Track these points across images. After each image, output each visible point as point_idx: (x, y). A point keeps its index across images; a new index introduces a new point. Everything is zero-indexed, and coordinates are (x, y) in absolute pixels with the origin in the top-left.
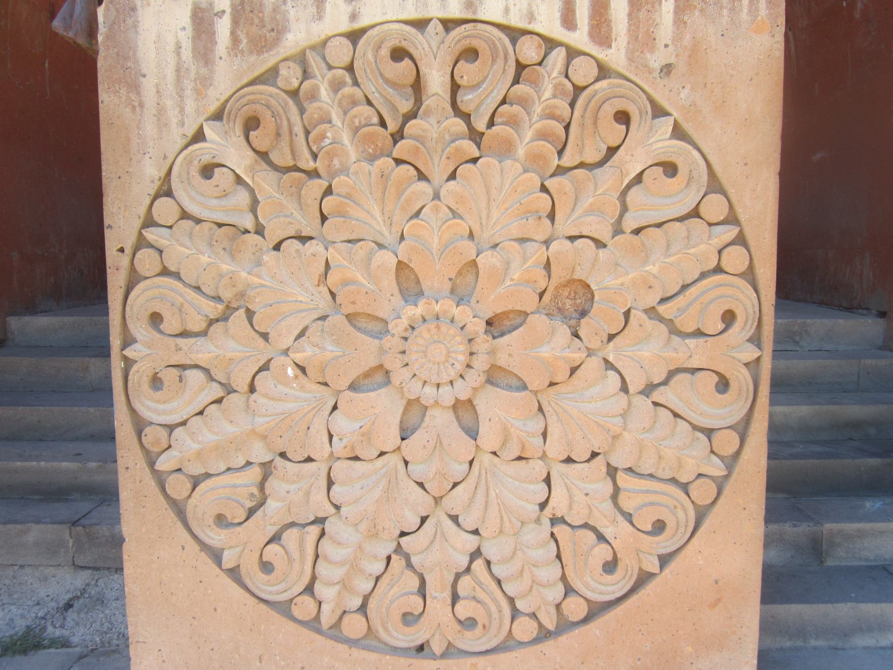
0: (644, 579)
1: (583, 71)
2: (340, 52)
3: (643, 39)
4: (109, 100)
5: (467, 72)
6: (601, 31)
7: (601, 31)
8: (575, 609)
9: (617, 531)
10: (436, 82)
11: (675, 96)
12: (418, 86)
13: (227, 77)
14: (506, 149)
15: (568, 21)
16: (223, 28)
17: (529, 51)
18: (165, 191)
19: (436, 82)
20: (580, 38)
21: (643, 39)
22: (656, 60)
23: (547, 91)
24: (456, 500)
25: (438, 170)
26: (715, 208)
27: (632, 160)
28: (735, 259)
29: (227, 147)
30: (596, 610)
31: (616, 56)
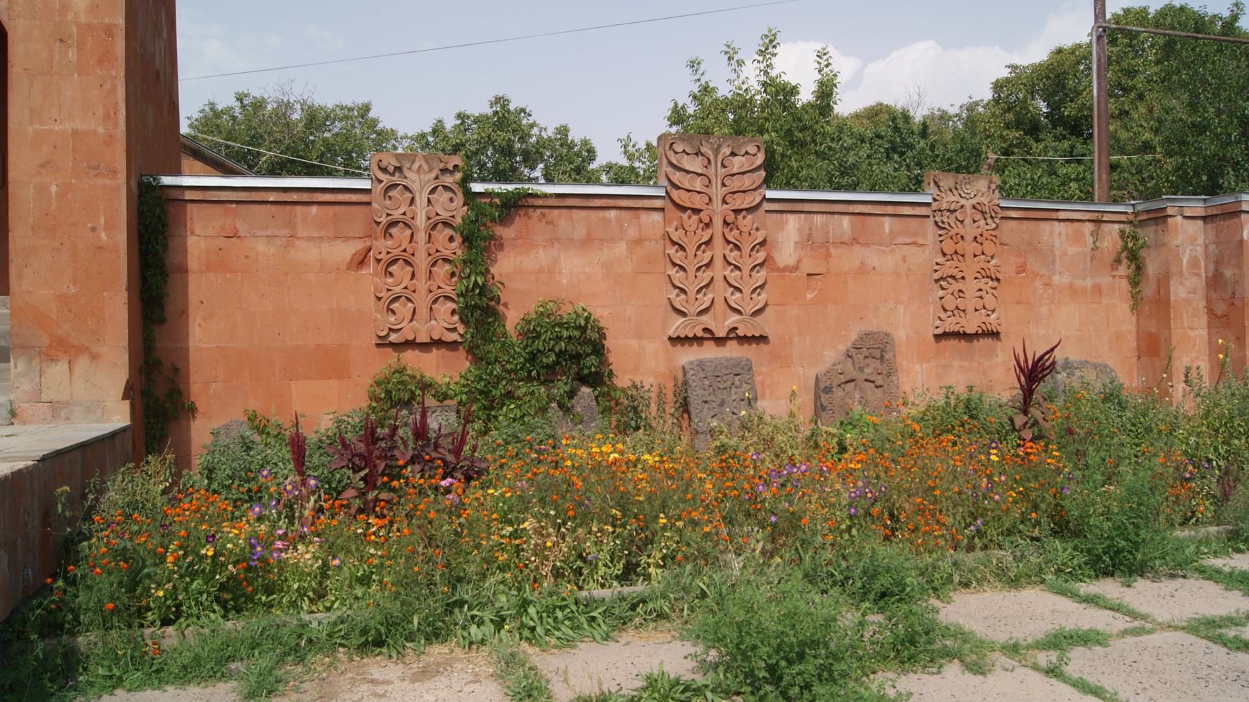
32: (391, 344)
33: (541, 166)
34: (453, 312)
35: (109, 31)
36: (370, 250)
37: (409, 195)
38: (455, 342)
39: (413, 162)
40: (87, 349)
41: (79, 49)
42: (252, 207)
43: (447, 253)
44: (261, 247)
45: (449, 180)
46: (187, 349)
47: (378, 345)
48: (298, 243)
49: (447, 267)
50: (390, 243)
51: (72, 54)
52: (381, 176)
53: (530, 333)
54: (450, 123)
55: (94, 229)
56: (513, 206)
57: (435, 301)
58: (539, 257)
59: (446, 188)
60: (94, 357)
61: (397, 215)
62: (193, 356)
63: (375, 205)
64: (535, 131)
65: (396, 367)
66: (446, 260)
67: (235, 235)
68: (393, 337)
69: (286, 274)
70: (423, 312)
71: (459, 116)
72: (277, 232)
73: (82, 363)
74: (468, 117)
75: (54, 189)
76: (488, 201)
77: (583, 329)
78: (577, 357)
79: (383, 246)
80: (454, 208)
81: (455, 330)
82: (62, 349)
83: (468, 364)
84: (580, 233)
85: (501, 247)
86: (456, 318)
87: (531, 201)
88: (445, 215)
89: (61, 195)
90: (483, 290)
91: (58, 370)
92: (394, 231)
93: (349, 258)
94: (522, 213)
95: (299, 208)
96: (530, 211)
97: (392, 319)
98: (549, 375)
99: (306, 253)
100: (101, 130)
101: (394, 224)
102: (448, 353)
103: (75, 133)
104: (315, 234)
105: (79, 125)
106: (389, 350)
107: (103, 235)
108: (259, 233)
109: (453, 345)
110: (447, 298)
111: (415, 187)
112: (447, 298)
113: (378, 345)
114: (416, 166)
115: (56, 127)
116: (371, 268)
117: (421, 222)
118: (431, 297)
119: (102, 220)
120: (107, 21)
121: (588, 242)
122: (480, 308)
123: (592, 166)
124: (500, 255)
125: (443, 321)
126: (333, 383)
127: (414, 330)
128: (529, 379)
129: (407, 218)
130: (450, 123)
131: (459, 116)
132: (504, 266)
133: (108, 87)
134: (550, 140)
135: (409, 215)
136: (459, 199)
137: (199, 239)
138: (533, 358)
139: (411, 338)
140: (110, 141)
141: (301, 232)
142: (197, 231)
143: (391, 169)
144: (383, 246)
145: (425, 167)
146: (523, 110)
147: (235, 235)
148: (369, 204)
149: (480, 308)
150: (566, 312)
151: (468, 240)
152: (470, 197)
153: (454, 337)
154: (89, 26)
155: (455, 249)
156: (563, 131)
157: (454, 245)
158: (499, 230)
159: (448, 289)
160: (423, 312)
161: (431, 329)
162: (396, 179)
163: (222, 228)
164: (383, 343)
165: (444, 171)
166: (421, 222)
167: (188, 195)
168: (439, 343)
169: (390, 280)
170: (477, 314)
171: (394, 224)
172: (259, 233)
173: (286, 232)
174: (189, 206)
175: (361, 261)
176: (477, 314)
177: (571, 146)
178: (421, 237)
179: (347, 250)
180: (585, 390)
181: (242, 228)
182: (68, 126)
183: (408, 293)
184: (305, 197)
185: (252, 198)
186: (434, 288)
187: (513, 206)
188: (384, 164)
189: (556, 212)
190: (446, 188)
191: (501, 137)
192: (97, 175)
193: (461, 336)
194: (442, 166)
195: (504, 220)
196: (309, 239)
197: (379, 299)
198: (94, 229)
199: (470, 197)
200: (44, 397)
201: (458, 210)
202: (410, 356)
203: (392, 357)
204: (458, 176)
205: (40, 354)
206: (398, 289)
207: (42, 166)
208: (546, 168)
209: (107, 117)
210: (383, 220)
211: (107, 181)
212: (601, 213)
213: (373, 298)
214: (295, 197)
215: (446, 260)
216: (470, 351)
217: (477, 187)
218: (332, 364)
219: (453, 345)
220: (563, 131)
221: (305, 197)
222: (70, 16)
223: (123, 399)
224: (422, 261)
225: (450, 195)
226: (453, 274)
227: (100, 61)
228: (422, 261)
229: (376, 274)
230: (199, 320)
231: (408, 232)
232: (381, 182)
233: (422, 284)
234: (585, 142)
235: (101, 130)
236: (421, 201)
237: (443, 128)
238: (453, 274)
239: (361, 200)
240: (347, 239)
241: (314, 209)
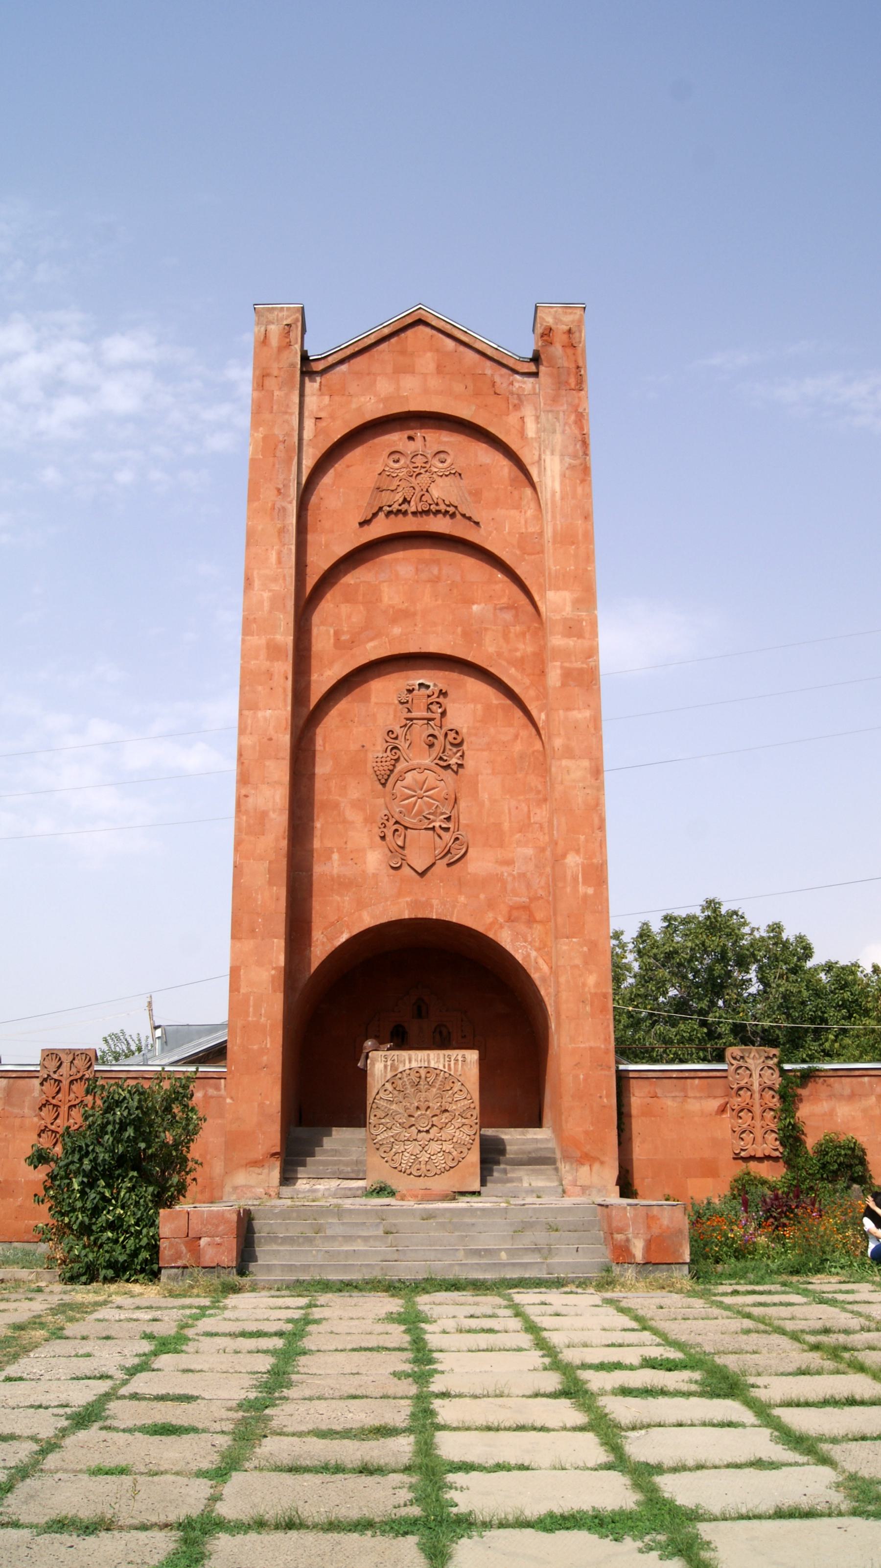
0: (459, 1161)
1: (447, 1075)
2: (408, 1072)
3: (456, 1070)
4: (369, 1079)
5: (428, 1075)
6: (450, 1069)
7: (450, 1069)
8: (447, 1168)
9: (455, 1153)
10: (423, 1076)
11: (461, 1079)
12: (420, 1077)
13: (389, 1077)
14: (435, 1087)
15: (444, 1067)
16: (389, 1068)
17: (438, 1072)
18: (378, 1093)
19: (423, 1076)
20: (446, 1070)
21: (456, 1070)
22: (459, 1073)
23: (440, 1079)
24: (426, 1149)
25: (423, 1091)
26: (469, 1098)
27: (456, 1089)
28: (472, 1106)
29: (388, 1086)
30: (451, 1167)
31: (452, 1073)
32: (742, 1158)
33: (754, 967)
34: (776, 1139)
35: (605, 996)
36: (727, 1103)
37: (748, 1072)
38: (778, 1157)
39: (750, 1053)
40: (598, 1159)
41: (592, 1006)
42: (664, 1080)
43: (771, 1105)
44: (670, 1103)
45: (771, 1063)
46: (632, 1160)
47: (734, 1159)
48: (689, 1100)
49: (772, 1113)
50: (739, 1099)
51: (588, 1008)
52: (734, 1062)
53: (822, 1151)
54: (657, 926)
55: (601, 1097)
56: (807, 1077)
57: (765, 1133)
58: (824, 1106)
59: (769, 1068)
60: (602, 1163)
61: (742, 1083)
62: (636, 1164)
63: (730, 1078)
64: (746, 930)
65: (746, 1171)
66: (771, 1109)
67: (655, 1096)
68: (743, 1154)
69: (682, 1118)
70: (759, 1139)
71: (666, 918)
72: (677, 1094)
73: (596, 1166)
74: (675, 919)
75: (582, 1077)
76: (792, 1074)
77: (853, 1150)
78: (850, 1166)
79: (736, 1102)
80: (774, 1079)
81: (777, 1150)
82: (586, 1159)
83: (785, 1170)
84: (847, 1091)
85: (801, 1100)
86: (778, 1143)
87: (817, 1073)
88: (769, 1083)
89: (585, 1080)
90: (794, 1127)
91: (585, 1169)
92: (741, 1092)
93: (716, 1108)
94: (812, 1080)
95: (689, 1080)
96: (817, 1079)
97: (742, 1143)
98: (833, 1177)
99: (694, 1106)
100: (603, 1046)
101: (740, 1089)
102: (773, 1163)
103: (591, 1048)
104: (698, 1095)
105: (592, 1044)
106: (740, 1161)
107: (605, 1100)
108: (668, 1095)
109: (776, 1159)
110: (773, 1131)
111: (752, 1067)
112: (773, 1131)
113: (734, 1159)
114: (752, 1055)
115: (582, 1045)
116: (728, 1114)
117: (756, 1087)
118: (763, 1130)
119: (605, 1092)
120: (604, 991)
121: (852, 1097)
122: (791, 1137)
123: (809, 964)
124: (801, 1106)
125: (771, 1145)
126: (710, 1180)
127: (755, 1150)
128: (822, 1179)
129: (748, 1086)
130: (657, 926)
131: (666, 918)
132: (804, 1111)
133: (605, 1024)
134: (762, 939)
135: (750, 1083)
136: (777, 1074)
137: (637, 1099)
138: (824, 1166)
139: (753, 1154)
140: (607, 1052)
141: (690, 1094)
142: (636, 1094)
143: (738, 1057)
144: (736, 1102)
145: (757, 1056)
146: (735, 913)
147: (655, 1096)
148: (726, 1077)
149: (791, 1137)
150: (843, 1139)
151: (783, 1097)
152: (783, 1072)
153: (777, 1154)
154: (596, 994)
155: (775, 1102)
156: (776, 928)
157: (775, 1100)
158: (800, 1091)
159: (773, 1126)
160: (759, 1139)
161: (764, 1149)
162: (741, 1063)
163: (649, 1092)
164: (737, 1157)
165: (768, 1058)
166: (756, 1087)
167: (631, 1075)
168: (768, 1158)
169: (740, 1121)
170: (791, 1141)
171: (740, 1089)
172: (668, 1095)
173: (682, 1094)
174: (632, 1081)
175: (722, 1110)
176: (791, 1141)
177: (785, 945)
178: (757, 1096)
179: (714, 1104)
180: (856, 1186)
181: (659, 1092)
182: (587, 1045)
183: (750, 1128)
184: (692, 1074)
185: (665, 1076)
186: (765, 1125)
187: (807, 1077)
188: (734, 1055)
189: (832, 1079)
190: (769, 1068)
191: (714, 942)
192: (602, 1069)
193: (781, 1153)
194: (766, 1055)
195: (803, 1085)
196: (695, 1098)
197: (734, 1132)
198: (601, 1097)
199: (783, 1072)
200: (578, 1183)
201: (776, 1080)
202: (752, 1165)
203: (743, 1165)
204: (775, 1060)
205: (577, 1161)
206: (745, 1126)
207: (576, 1065)
208: (761, 969)
209: (605, 1040)
210: (735, 1086)
211: (607, 1073)
212: (859, 1079)
213: (730, 1131)
214: (687, 1074)
215: (771, 1109)
216: (785, 1163)
217: (787, 1067)
218: (709, 1169)
219: (776, 1159)
220: (776, 928)
221: (692, 1074)
222: (587, 989)
223: (617, 1184)
224: (757, 1110)
225: (770, 1071)
226: (775, 1117)
227: (601, 1011)
228: (757, 1110)
229: (731, 1117)
230: (638, 1144)
231: (749, 1093)
232: (732, 1065)
233: (758, 1123)
234: (800, 939)
235: (603, 1046)
236: (756, 1076)
237: (649, 931)
238: (775, 1117)
239: (723, 1076)
240: (715, 1097)
241: (697, 1081)
